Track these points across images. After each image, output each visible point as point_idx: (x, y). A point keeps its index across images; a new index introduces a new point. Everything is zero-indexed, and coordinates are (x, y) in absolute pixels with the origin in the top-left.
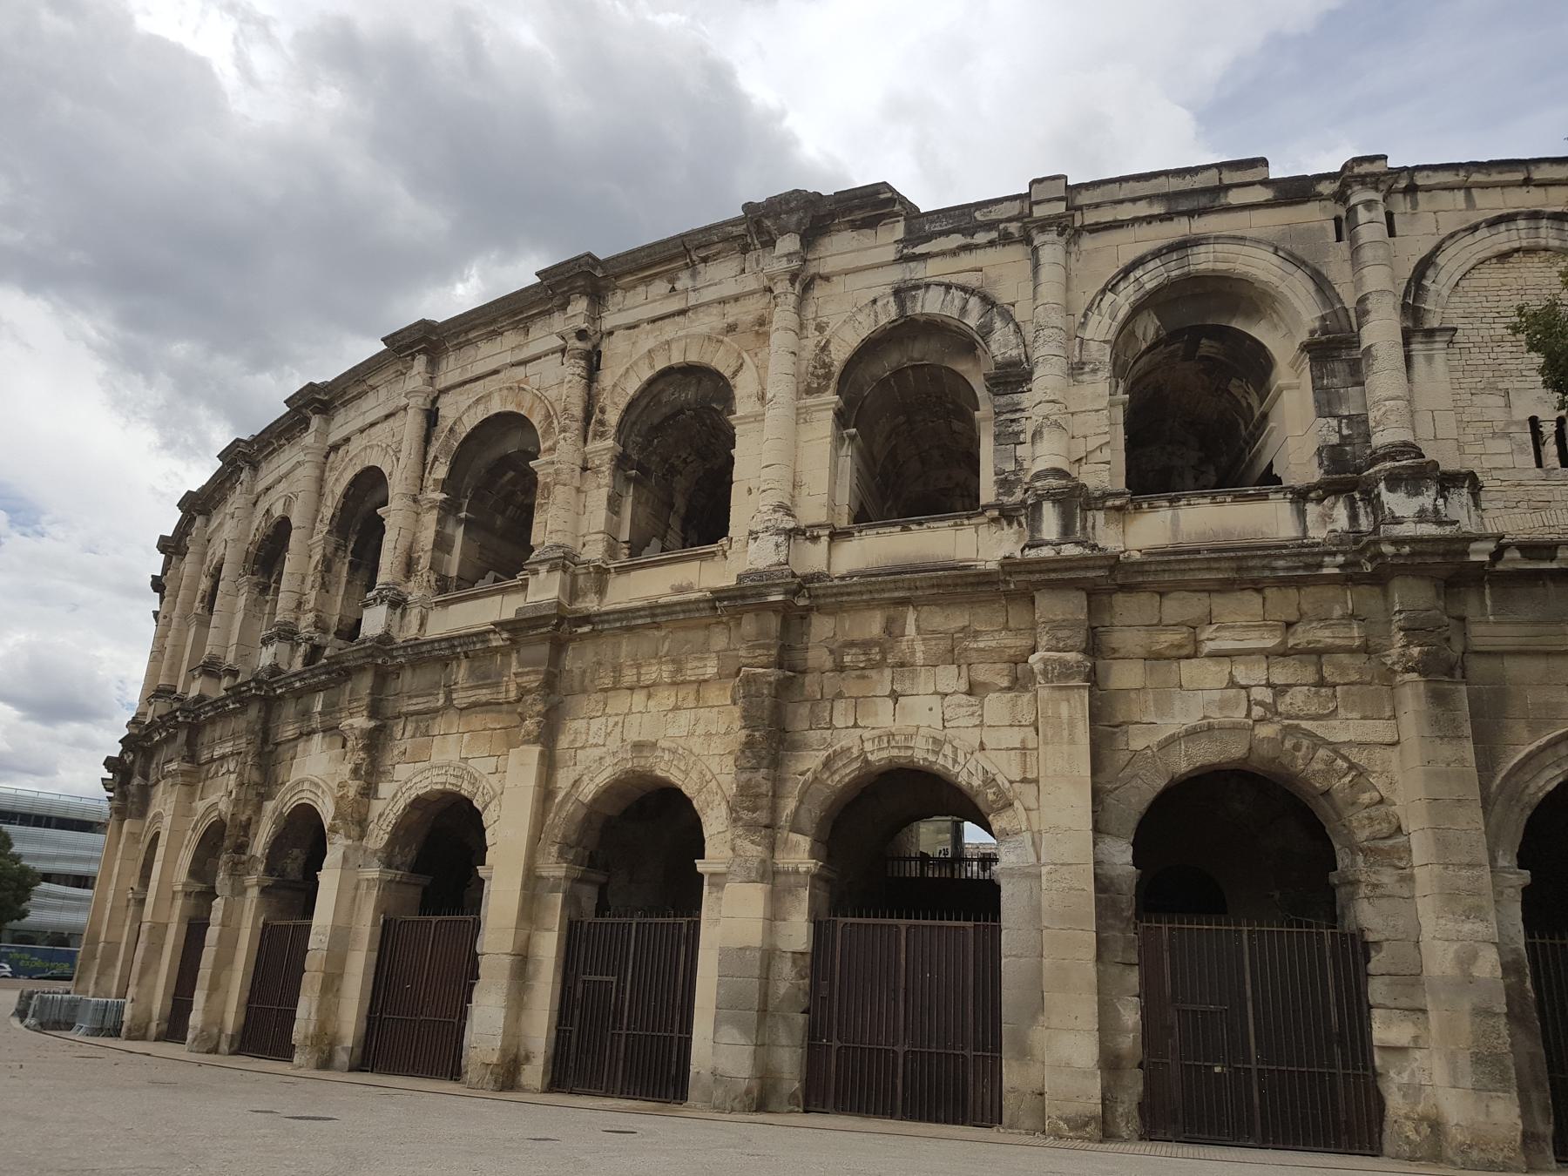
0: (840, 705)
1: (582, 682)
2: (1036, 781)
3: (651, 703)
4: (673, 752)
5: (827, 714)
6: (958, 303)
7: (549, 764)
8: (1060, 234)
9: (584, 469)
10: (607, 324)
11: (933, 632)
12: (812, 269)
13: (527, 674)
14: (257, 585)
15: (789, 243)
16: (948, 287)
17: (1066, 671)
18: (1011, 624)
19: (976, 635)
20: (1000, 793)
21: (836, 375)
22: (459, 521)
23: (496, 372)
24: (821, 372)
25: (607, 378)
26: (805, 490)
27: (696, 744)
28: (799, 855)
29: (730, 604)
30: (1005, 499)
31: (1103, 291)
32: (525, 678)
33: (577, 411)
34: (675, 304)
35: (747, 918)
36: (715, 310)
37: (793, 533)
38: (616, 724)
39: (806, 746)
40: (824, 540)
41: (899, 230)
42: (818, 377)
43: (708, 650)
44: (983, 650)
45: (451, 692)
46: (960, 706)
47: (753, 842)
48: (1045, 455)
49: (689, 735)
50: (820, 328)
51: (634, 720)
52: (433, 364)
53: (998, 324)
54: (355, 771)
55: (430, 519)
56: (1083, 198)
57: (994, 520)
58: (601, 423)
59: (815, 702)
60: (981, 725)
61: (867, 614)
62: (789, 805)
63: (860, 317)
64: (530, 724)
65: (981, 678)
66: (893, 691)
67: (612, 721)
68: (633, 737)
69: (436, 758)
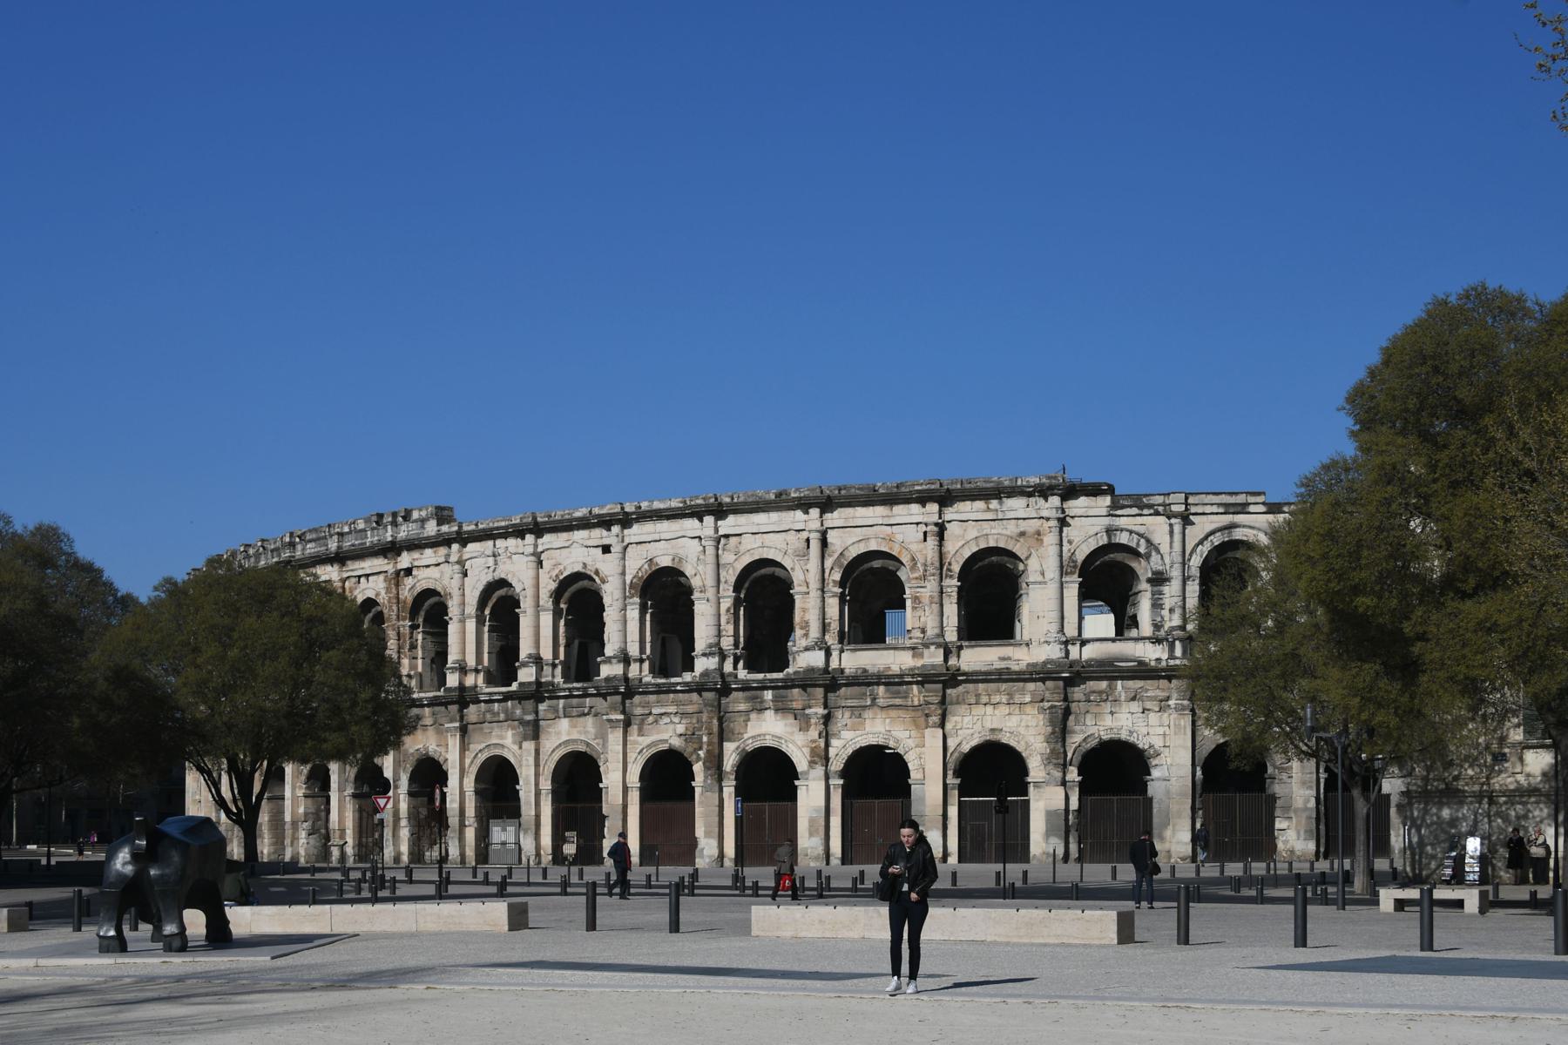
0: (1089, 716)
10: (947, 517)
25: (950, 546)
28: (1073, 775)
34: (990, 516)
35: (1048, 800)
37: (1066, 643)
39: (1074, 732)
49: (1024, 728)
68: (989, 725)
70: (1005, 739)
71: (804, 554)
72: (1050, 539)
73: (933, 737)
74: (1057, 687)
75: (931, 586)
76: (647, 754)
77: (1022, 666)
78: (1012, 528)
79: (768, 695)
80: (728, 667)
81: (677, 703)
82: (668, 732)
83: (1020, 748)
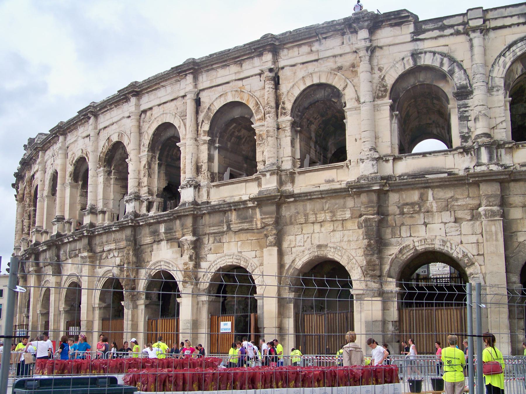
0: (403, 228)
1: (291, 220)
2: (483, 255)
3: (323, 229)
4: (335, 248)
5: (398, 232)
6: (439, 60)
7: (281, 254)
8: (481, 33)
9: (278, 129)
10: (281, 64)
11: (439, 199)
12: (375, 44)
13: (267, 218)
14: (106, 172)
15: (364, 34)
16: (434, 53)
17: (493, 214)
18: (470, 195)
19: (457, 200)
20: (469, 259)
21: (389, 91)
22: (215, 148)
23: (228, 83)
24: (383, 89)
25: (284, 88)
26: (380, 140)
27: (344, 245)
29: (355, 189)
30: (464, 144)
31: (500, 56)
32: (267, 220)
33: (273, 104)
36: (332, 60)
38: (308, 237)
40: (391, 161)
41: (411, 28)
42: (381, 91)
43: (345, 208)
44: (460, 205)
45: (230, 225)
46: (452, 227)
47: (374, 282)
48: (479, 128)
50: (380, 70)
51: (316, 235)
52: (196, 79)
53: (456, 70)
54: (191, 258)
55: (204, 148)
56: (489, 15)
57: (461, 153)
58: (283, 108)
59: (393, 228)
60: (461, 234)
61: (412, 192)
62: (386, 268)
63: (397, 65)
64: (271, 238)
65: (460, 216)
66: (425, 222)
67: (306, 236)
68: (316, 242)
69: (226, 251)
70: (331, 255)
71: (183, 116)
72: (363, 67)
73: (271, 255)
74: (370, 201)
75: (270, 122)
76: (103, 281)
77: (343, 185)
78: (331, 64)
79: (162, 228)
80: (144, 211)
81: (116, 241)
82: (112, 265)
83: (343, 263)
